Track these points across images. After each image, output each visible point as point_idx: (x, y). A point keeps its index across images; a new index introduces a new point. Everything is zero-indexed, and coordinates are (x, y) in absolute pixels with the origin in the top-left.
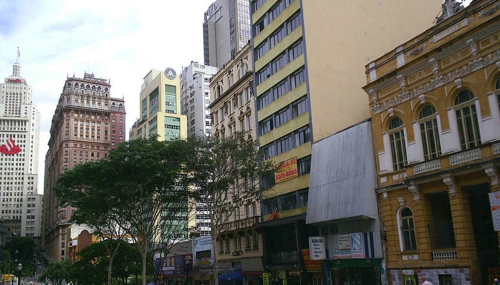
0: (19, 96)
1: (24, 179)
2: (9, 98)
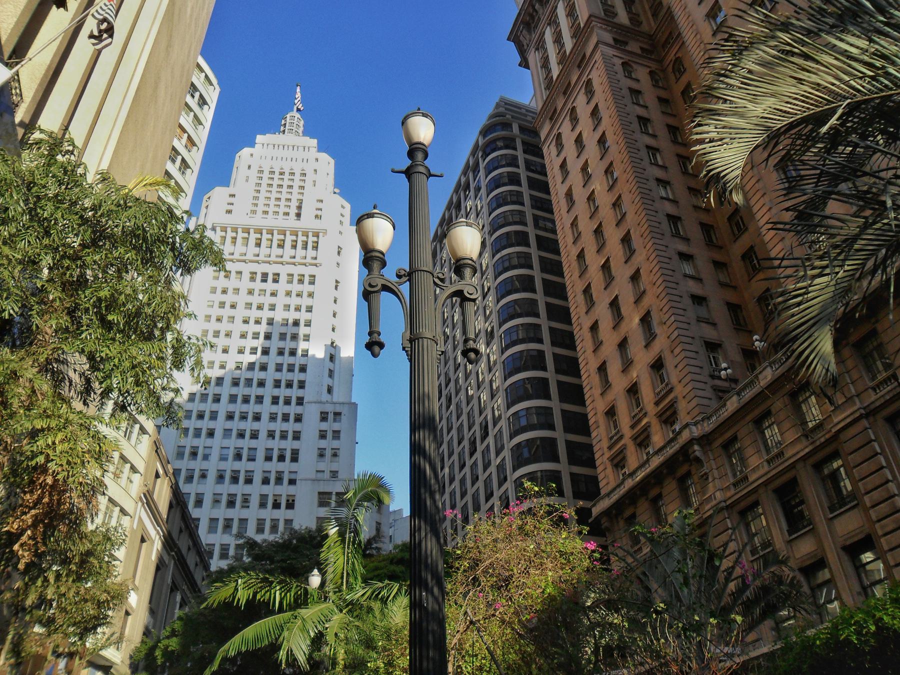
0: (297, 177)
1: (303, 436)
2: (265, 181)
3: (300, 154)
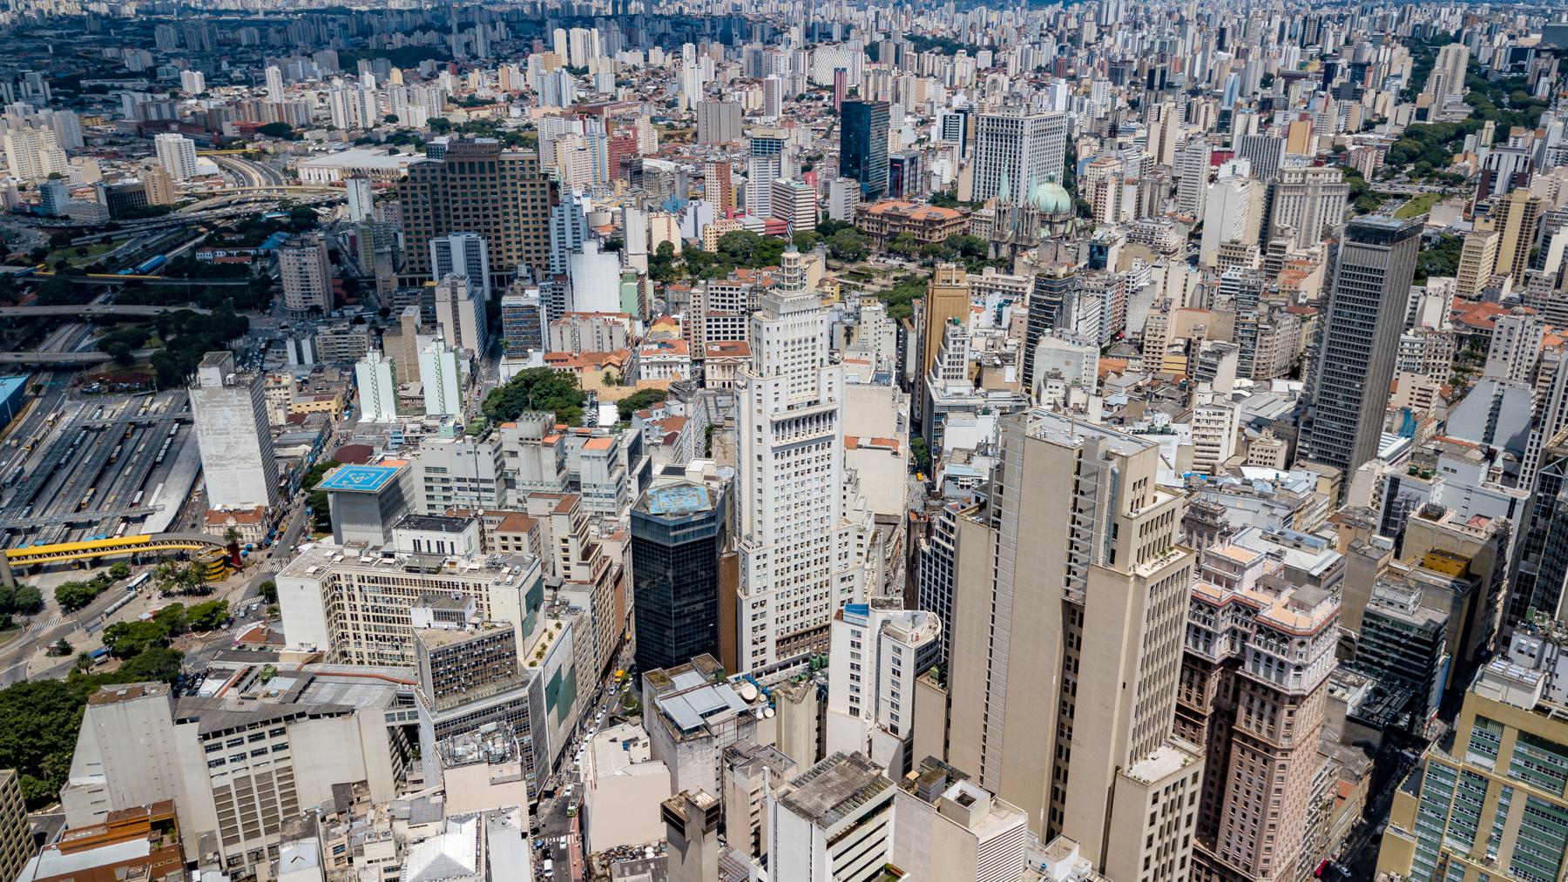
3: (810, 317)
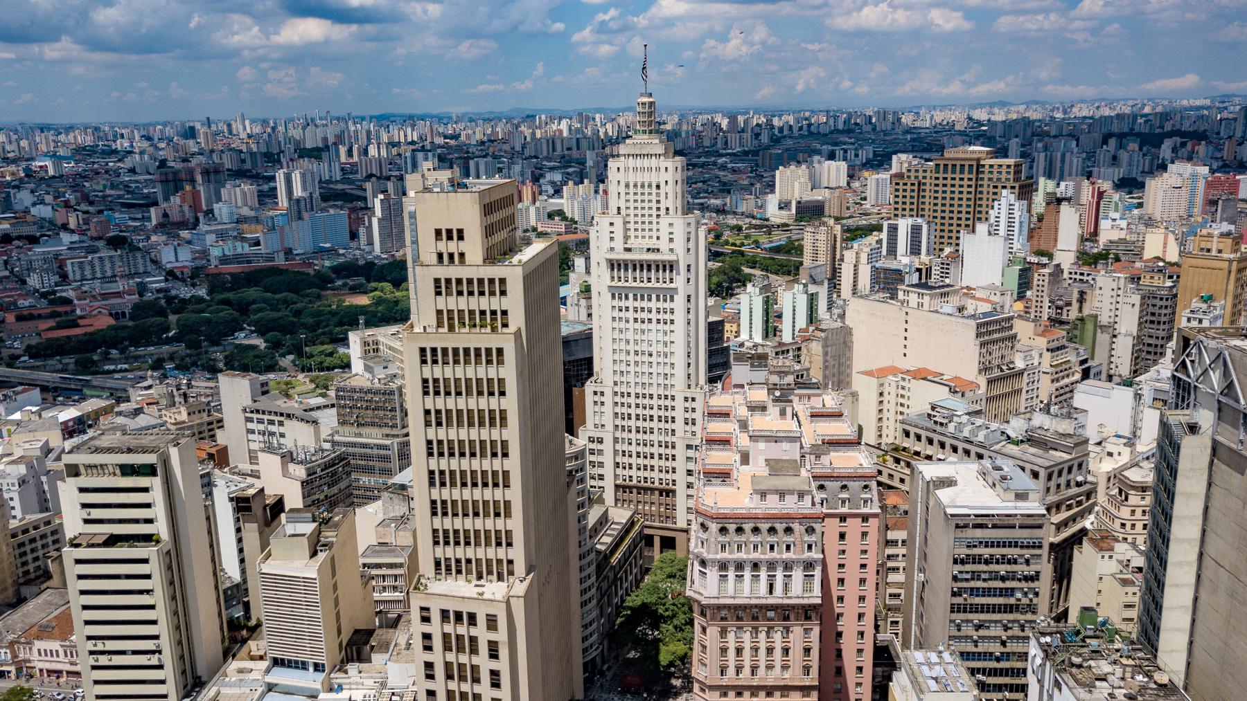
3: (654, 162)
